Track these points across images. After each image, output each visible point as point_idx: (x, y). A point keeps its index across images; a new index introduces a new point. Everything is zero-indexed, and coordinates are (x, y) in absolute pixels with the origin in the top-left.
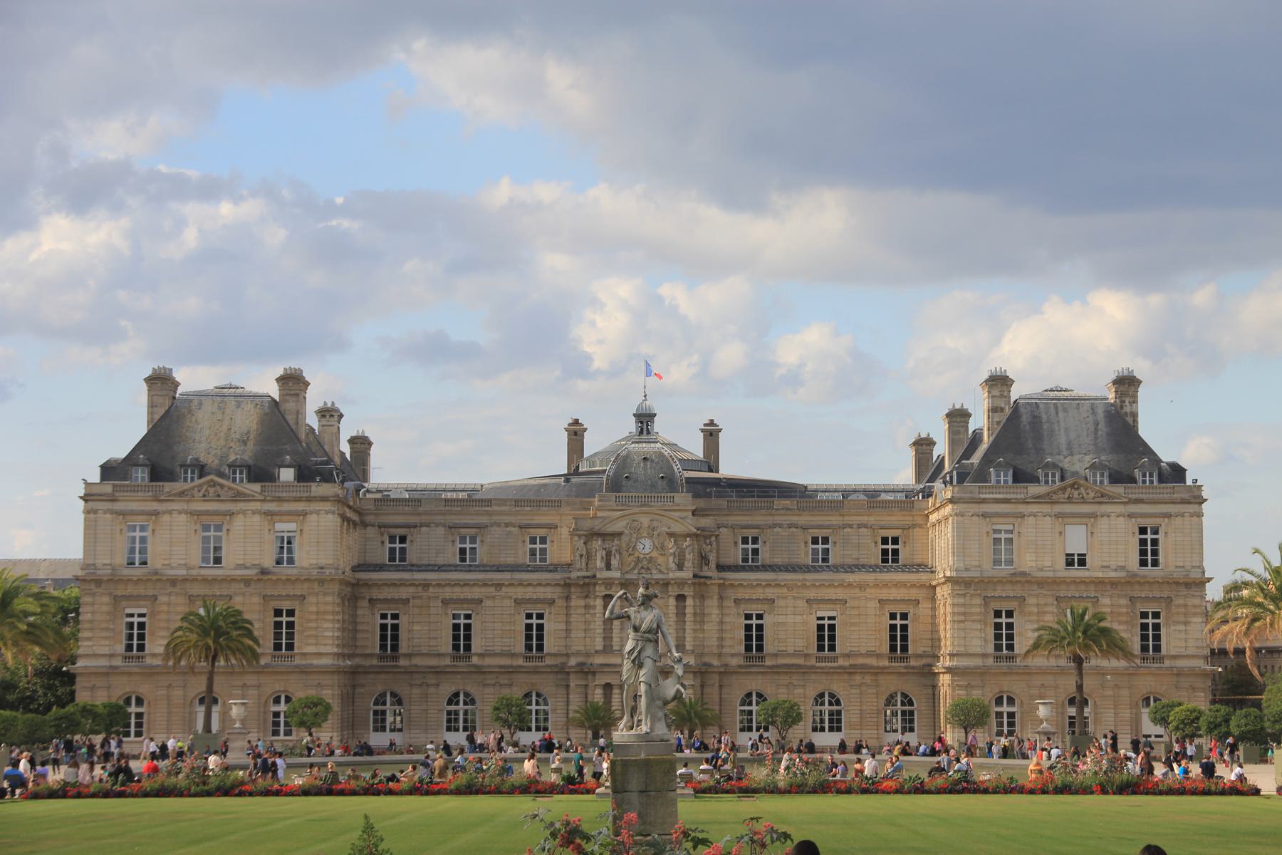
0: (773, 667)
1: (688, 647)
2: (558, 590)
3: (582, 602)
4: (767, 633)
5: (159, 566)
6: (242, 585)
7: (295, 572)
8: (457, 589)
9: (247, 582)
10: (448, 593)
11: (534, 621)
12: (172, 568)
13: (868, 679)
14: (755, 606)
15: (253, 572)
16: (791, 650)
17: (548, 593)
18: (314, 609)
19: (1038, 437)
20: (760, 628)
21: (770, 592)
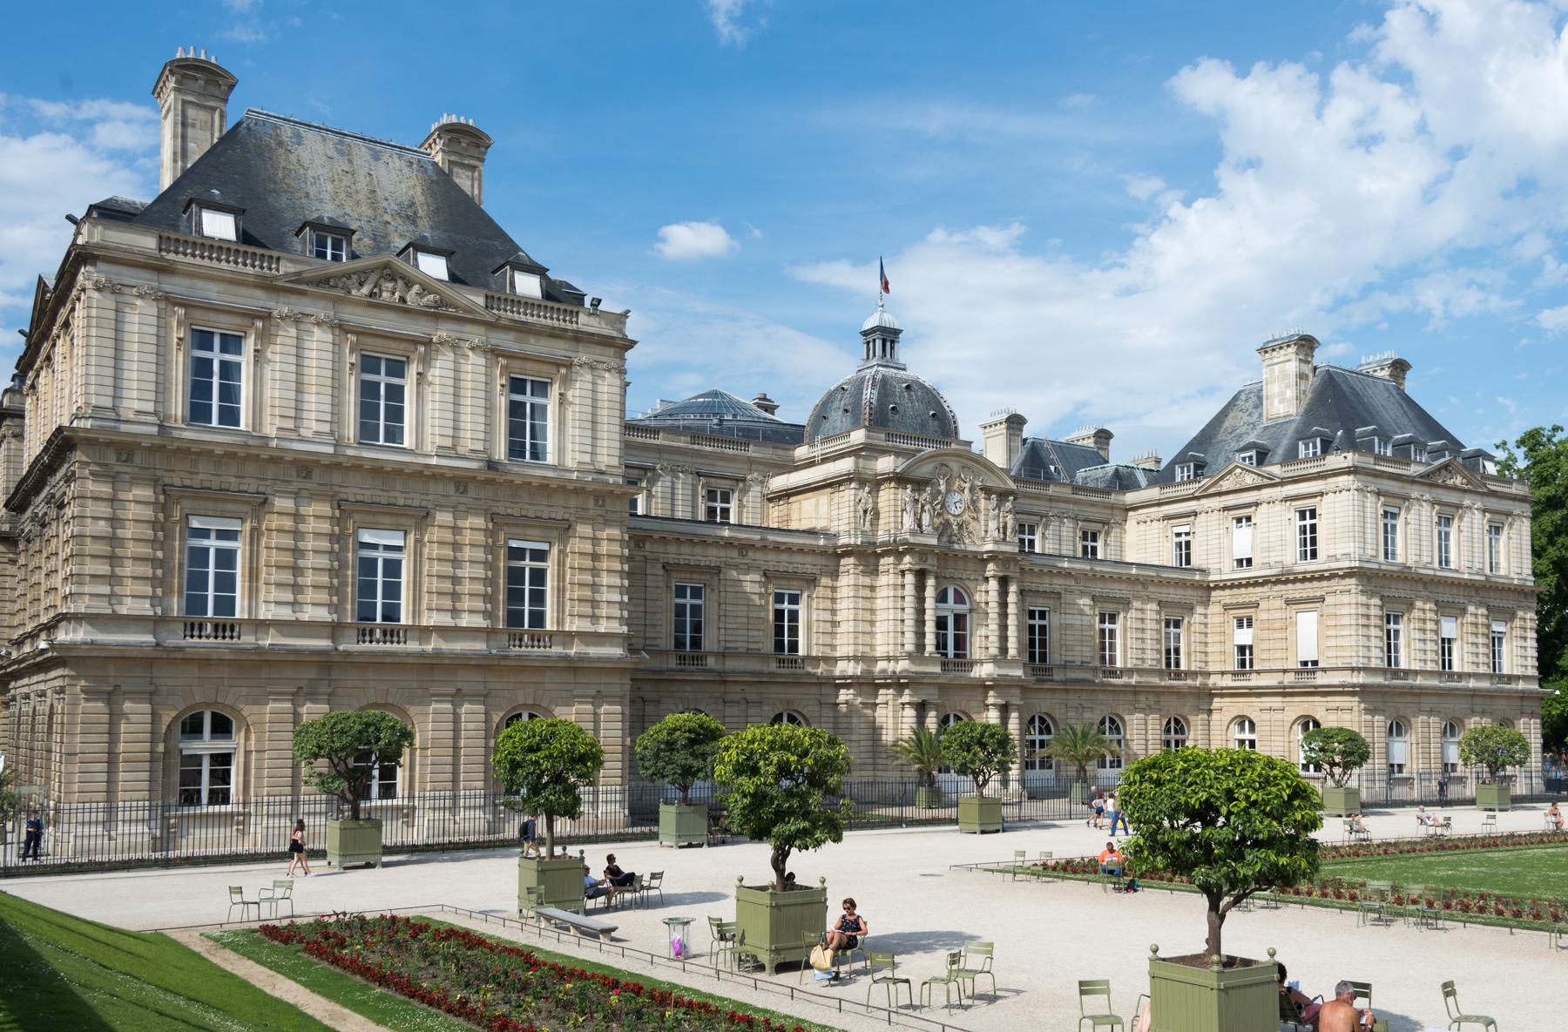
0: (1065, 682)
1: (1012, 652)
2: (820, 560)
3: (867, 581)
4: (1053, 637)
5: (270, 430)
6: (451, 490)
7: (550, 474)
8: (685, 549)
9: (461, 481)
10: (672, 553)
11: (786, 606)
12: (302, 440)
13: (1152, 698)
14: (1040, 600)
15: (474, 465)
16: (1078, 660)
17: (807, 564)
18: (588, 547)
19: (1367, 410)
20: (1043, 629)
21: (1058, 584)
